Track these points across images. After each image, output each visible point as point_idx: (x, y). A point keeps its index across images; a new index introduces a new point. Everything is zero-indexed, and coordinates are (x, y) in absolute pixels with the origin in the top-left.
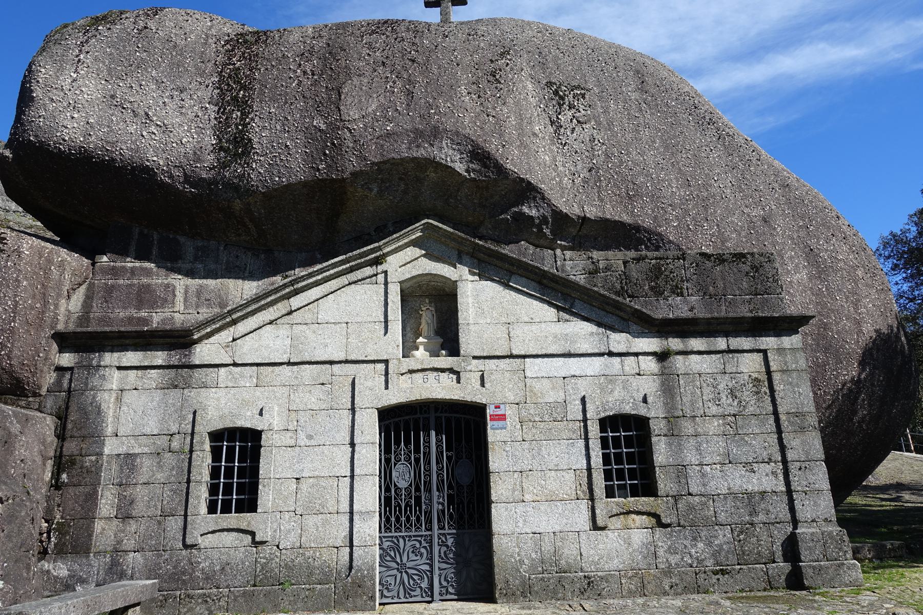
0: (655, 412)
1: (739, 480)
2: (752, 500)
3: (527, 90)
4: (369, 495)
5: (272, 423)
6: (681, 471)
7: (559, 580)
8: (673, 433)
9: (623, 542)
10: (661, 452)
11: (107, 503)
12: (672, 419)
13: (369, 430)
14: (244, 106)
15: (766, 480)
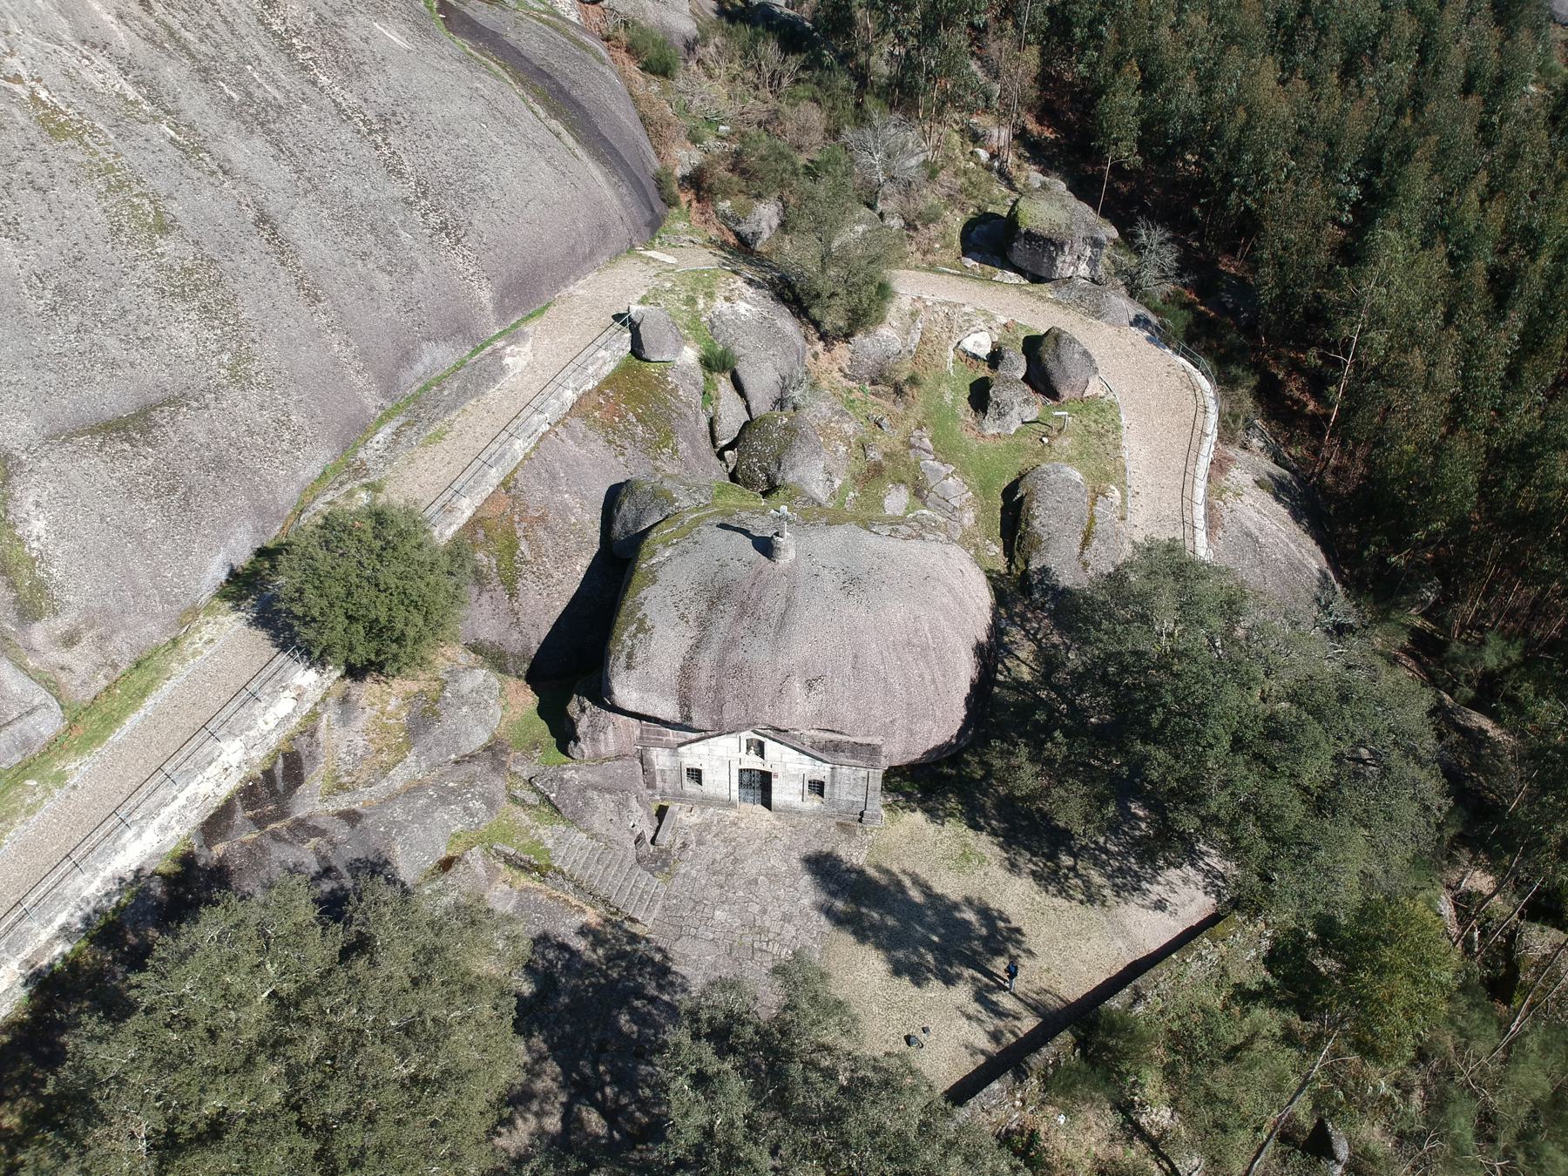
0: (827, 782)
1: (851, 798)
2: (853, 803)
3: (797, 687)
4: (735, 786)
5: (705, 769)
6: (833, 794)
7: (789, 811)
8: (833, 784)
9: (813, 803)
10: (827, 789)
11: (658, 779)
12: (833, 784)
13: (735, 775)
14: (689, 707)
15: (861, 799)
